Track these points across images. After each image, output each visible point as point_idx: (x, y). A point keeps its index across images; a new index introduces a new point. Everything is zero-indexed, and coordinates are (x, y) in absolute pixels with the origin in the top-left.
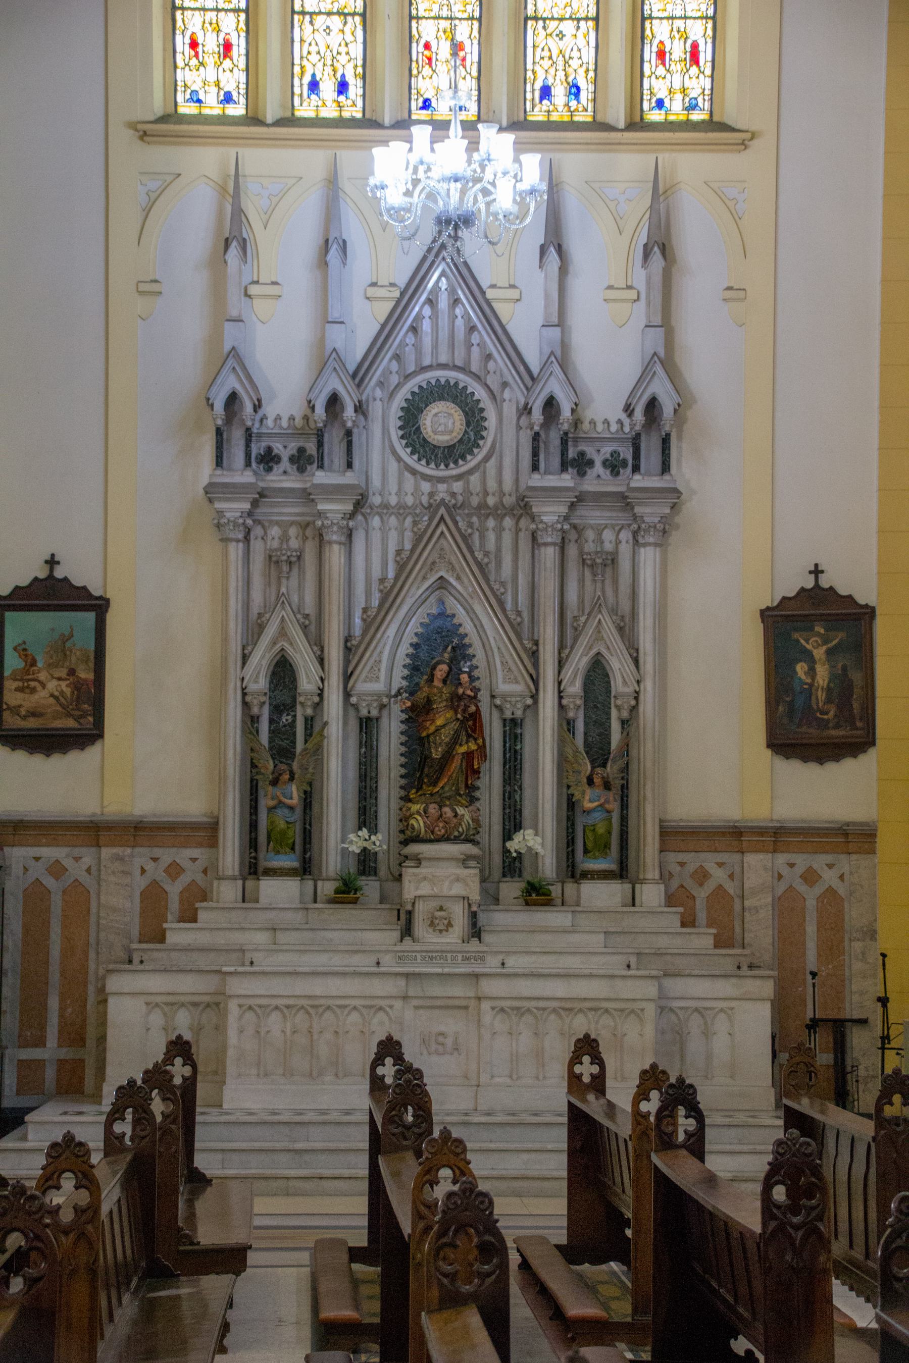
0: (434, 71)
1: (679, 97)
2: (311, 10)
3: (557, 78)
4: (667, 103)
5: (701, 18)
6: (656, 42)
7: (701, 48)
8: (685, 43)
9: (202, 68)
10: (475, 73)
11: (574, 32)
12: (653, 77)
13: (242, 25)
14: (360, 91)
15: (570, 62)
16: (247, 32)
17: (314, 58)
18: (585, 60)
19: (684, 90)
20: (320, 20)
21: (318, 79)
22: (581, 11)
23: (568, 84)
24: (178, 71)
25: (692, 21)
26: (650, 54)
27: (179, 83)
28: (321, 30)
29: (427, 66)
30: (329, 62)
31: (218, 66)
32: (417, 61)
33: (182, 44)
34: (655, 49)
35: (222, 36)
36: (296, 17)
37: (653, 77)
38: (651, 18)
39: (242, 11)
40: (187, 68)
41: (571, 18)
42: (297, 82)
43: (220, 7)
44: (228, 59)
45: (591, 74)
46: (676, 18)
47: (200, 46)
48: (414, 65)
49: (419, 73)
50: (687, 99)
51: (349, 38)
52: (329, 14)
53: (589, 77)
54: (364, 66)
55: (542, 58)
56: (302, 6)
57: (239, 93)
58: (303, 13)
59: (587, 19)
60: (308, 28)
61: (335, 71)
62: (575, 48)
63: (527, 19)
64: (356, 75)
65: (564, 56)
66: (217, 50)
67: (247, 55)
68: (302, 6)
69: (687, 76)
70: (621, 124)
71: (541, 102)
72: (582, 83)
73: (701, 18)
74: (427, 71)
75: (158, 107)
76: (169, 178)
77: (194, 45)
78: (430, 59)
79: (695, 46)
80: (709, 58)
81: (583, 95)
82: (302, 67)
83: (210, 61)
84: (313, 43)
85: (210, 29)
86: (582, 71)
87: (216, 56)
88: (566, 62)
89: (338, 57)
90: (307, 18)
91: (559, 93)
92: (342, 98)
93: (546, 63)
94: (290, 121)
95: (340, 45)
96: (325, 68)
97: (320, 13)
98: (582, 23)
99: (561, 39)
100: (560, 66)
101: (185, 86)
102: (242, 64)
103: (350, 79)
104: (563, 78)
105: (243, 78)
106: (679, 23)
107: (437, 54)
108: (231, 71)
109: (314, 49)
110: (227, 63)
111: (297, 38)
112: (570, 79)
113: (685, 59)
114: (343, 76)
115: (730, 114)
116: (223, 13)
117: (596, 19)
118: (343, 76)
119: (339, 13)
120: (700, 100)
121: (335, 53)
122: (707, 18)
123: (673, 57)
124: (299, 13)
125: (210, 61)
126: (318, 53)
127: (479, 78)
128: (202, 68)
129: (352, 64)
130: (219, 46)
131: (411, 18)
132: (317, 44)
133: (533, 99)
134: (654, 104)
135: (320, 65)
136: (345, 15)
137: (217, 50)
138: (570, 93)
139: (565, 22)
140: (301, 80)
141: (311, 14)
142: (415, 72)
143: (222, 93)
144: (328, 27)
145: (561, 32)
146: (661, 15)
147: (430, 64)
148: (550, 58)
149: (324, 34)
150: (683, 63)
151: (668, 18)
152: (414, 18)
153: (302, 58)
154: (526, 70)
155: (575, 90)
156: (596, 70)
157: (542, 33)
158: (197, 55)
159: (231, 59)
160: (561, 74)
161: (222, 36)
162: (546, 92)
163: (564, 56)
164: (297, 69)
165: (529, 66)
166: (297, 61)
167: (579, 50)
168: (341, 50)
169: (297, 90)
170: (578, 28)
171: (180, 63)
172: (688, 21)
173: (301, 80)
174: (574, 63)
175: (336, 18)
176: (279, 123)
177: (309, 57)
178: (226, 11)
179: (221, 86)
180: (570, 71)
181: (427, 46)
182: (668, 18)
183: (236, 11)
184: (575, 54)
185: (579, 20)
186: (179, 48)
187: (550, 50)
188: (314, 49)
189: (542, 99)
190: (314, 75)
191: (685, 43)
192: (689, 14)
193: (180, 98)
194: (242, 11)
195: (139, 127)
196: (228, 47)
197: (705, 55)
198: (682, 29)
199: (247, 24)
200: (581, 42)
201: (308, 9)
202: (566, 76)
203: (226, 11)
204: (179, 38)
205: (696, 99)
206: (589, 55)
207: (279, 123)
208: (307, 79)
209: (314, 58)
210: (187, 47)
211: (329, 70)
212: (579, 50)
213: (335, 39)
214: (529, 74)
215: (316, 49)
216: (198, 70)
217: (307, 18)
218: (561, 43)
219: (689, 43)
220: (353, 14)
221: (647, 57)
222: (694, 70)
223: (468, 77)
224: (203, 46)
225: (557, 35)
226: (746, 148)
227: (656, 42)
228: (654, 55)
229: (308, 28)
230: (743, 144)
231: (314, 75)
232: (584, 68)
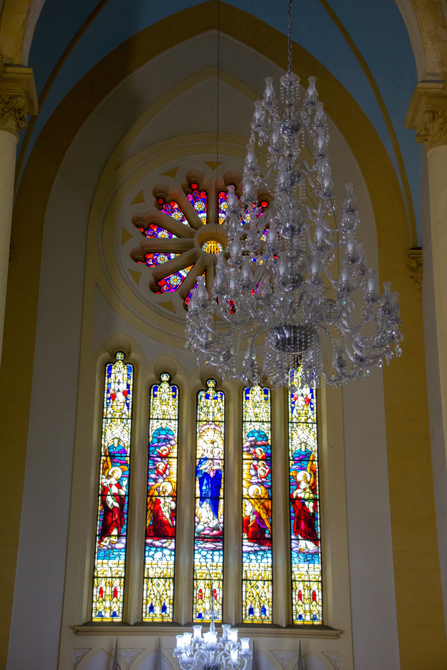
0: (203, 601)
1: (308, 614)
2: (152, 577)
3: (256, 605)
4: (303, 616)
5: (316, 581)
6: (298, 591)
7: (317, 593)
8: (310, 591)
9: (104, 602)
10: (221, 602)
11: (262, 585)
12: (297, 605)
13: (122, 583)
14: (171, 610)
15: (262, 598)
16: (124, 586)
17: (152, 596)
19: (310, 611)
20: (155, 581)
21: (153, 605)
22: (265, 577)
23: (261, 607)
24: (94, 603)
25: (312, 583)
26: (295, 596)
27: (94, 608)
28: (156, 585)
29: (200, 600)
30: (158, 598)
31: (111, 601)
32: (196, 597)
33: (96, 591)
34: (297, 593)
35: (113, 588)
36: (145, 580)
37: (297, 605)
38: (295, 581)
39: (122, 578)
40: (98, 602)
41: (261, 580)
42: (144, 606)
43: (113, 576)
44: (115, 598)
45: (271, 603)
46: (306, 581)
47: (104, 593)
48: (195, 599)
49: (197, 602)
50: (312, 615)
51: (167, 588)
52: (159, 578)
53: (270, 604)
54: (173, 600)
55: (249, 596)
56: (148, 575)
57: (119, 612)
58: (148, 578)
59: (268, 580)
60: (150, 584)
61: (161, 602)
62: (263, 592)
63: (243, 580)
64: (170, 604)
65: (259, 596)
67: (124, 596)
68: (148, 575)
69: (311, 605)
70: (284, 625)
71: (249, 615)
72: (267, 607)
73: (316, 581)
74: (200, 601)
75: (84, 618)
76: (86, 651)
77: (101, 591)
78: (201, 596)
79: (314, 593)
80: (320, 598)
81: (267, 613)
82: (147, 600)
83: (108, 598)
84: (152, 590)
86: (266, 602)
87: (110, 596)
88: (260, 598)
89: (163, 596)
90: (150, 580)
91: (257, 611)
92: (163, 613)
93: (251, 599)
94: (141, 623)
95: (163, 591)
97: (155, 578)
98: (266, 582)
99: (257, 589)
100: (257, 600)
101: (97, 610)
102: (121, 600)
103: (167, 605)
104: (259, 605)
105: (121, 605)
106: (306, 583)
108: (116, 603)
109: (152, 592)
110: (115, 600)
112: (262, 605)
113: (310, 598)
114: (164, 604)
115: (331, 622)
116: (114, 579)
117: (272, 581)
119: (163, 578)
120: (317, 616)
121: (161, 594)
122: (318, 581)
123: (305, 597)
124: (146, 578)
125: (108, 598)
126: (154, 594)
127: (222, 605)
128: (104, 602)
130: (112, 592)
131: (194, 579)
132: (153, 591)
133: (246, 614)
134: (298, 617)
135: (154, 599)
136: (166, 578)
137: (111, 594)
138: (262, 611)
139: (259, 582)
140: (146, 605)
141: (152, 578)
142: (195, 602)
143: (112, 612)
144: (159, 584)
145: (257, 586)
146: (299, 579)
147: (202, 599)
148: (253, 596)
149: (157, 586)
150: (310, 600)
151: (302, 581)
152: (195, 579)
153: (147, 597)
154: (242, 601)
155: (263, 610)
156: (272, 602)
157: (249, 586)
158: (102, 597)
159: (117, 598)
160: (257, 603)
161: (113, 588)
162: (251, 611)
163: (259, 596)
164: (145, 601)
165: (244, 599)
166: (145, 598)
167: (265, 593)
168: (164, 592)
169: (144, 610)
170: (264, 584)
171: (95, 600)
172: (311, 583)
173: (146, 605)
174: (263, 599)
175: (162, 580)
176: (136, 624)
177: (150, 596)
178: (116, 578)
179: (112, 608)
181: (201, 591)
182: (302, 581)
183: (120, 578)
184: (263, 595)
185: (264, 581)
186: (95, 594)
188: (152, 592)
189: (250, 613)
190: (152, 604)
191: (310, 591)
192: (311, 579)
193: (94, 615)
194: (122, 578)
195: (76, 628)
197: (319, 596)
198: (308, 586)
199: (124, 583)
200: (266, 590)
201: (151, 576)
202: (260, 604)
203: (116, 578)
204: (95, 590)
205: (316, 615)
206: (269, 596)
207: (136, 624)
208: (149, 605)
209: (152, 596)
210: (98, 593)
211: (158, 601)
212: (265, 593)
213: (161, 588)
214: (244, 603)
215: (153, 592)
216: (102, 603)
217: (150, 580)
218: (257, 591)
219: (312, 591)
220: (169, 578)
221: (294, 597)
222: (314, 603)
223: (218, 604)
224: (105, 592)
225: (256, 587)
226: (339, 637)
227: (298, 591)
228: (297, 597)
229: (150, 584)
230: (337, 635)
231: (152, 604)
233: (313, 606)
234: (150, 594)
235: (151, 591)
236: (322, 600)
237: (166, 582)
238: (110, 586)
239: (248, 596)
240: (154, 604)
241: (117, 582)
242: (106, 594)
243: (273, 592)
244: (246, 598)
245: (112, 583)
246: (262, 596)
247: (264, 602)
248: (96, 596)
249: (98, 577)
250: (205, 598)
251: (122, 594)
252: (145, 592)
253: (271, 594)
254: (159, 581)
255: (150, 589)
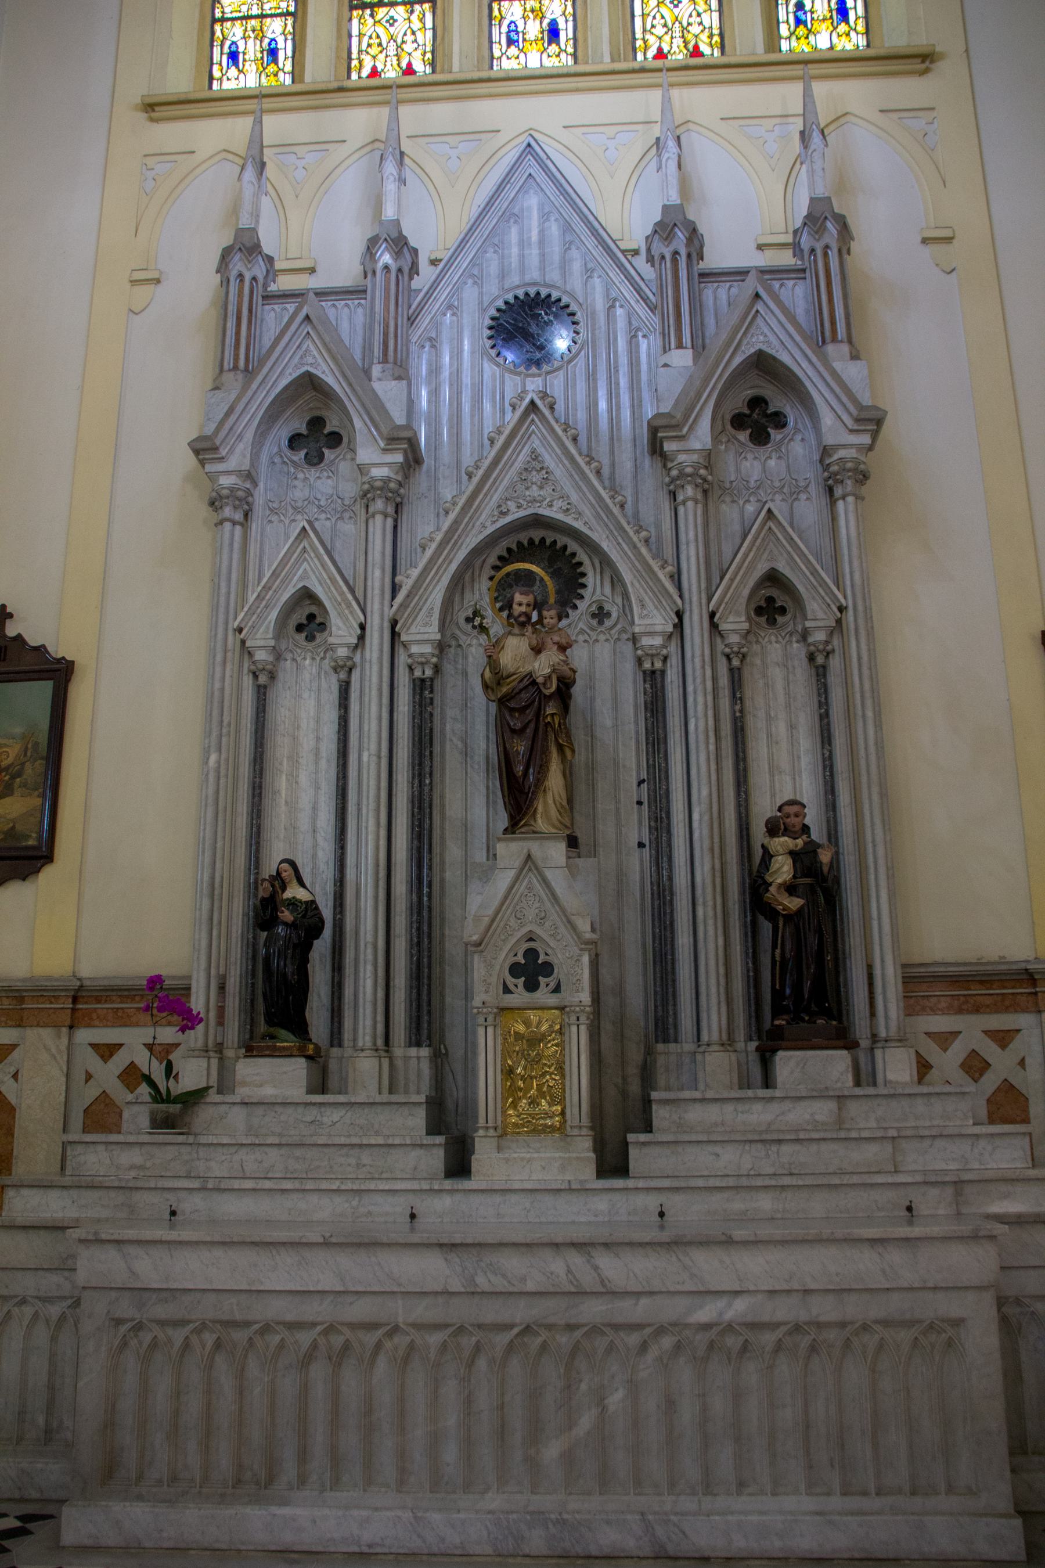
9: (242, 76)
17: (374, 50)
18: (707, 23)
21: (379, 70)
28: (383, 22)
45: (716, 39)
51: (416, 25)
53: (713, 42)
65: (680, 23)
66: (259, 55)
85: (252, 35)
86: (704, 37)
88: (683, 29)
96: (388, 59)
100: (677, 34)
104: (682, 45)
107: (524, 34)
111: (355, 32)
114: (409, 65)
116: (269, 20)
118: (409, 65)
126: (380, 45)
129: (420, 52)
132: (378, 37)
149: (387, 25)
153: (360, 52)
160: (678, 42)
161: (266, 41)
163: (680, 23)
164: (355, 63)
165: (639, 35)
177: (369, 50)
180: (689, 37)
187: (663, 17)
196: (273, 53)
203: (272, 16)
214: (639, 43)
215: (378, 41)
222: (843, 28)
224: (244, 54)
232: (707, 33)
233: (839, 36)
234: (369, 46)
235: (370, 37)
236: (866, 18)
237: (412, 12)
238: (256, 38)
239: (648, 27)
240: (380, 68)
241: (275, 28)
242: (247, 57)
243: (720, 11)
244: (644, 31)
245: (261, 30)
246: (689, 24)
247: (696, 37)
248: (221, 64)
249: (223, 20)
250: (527, 45)
251: (289, 53)
252: (355, 41)
253: (716, 16)
254: (392, 13)
255: (369, 34)
